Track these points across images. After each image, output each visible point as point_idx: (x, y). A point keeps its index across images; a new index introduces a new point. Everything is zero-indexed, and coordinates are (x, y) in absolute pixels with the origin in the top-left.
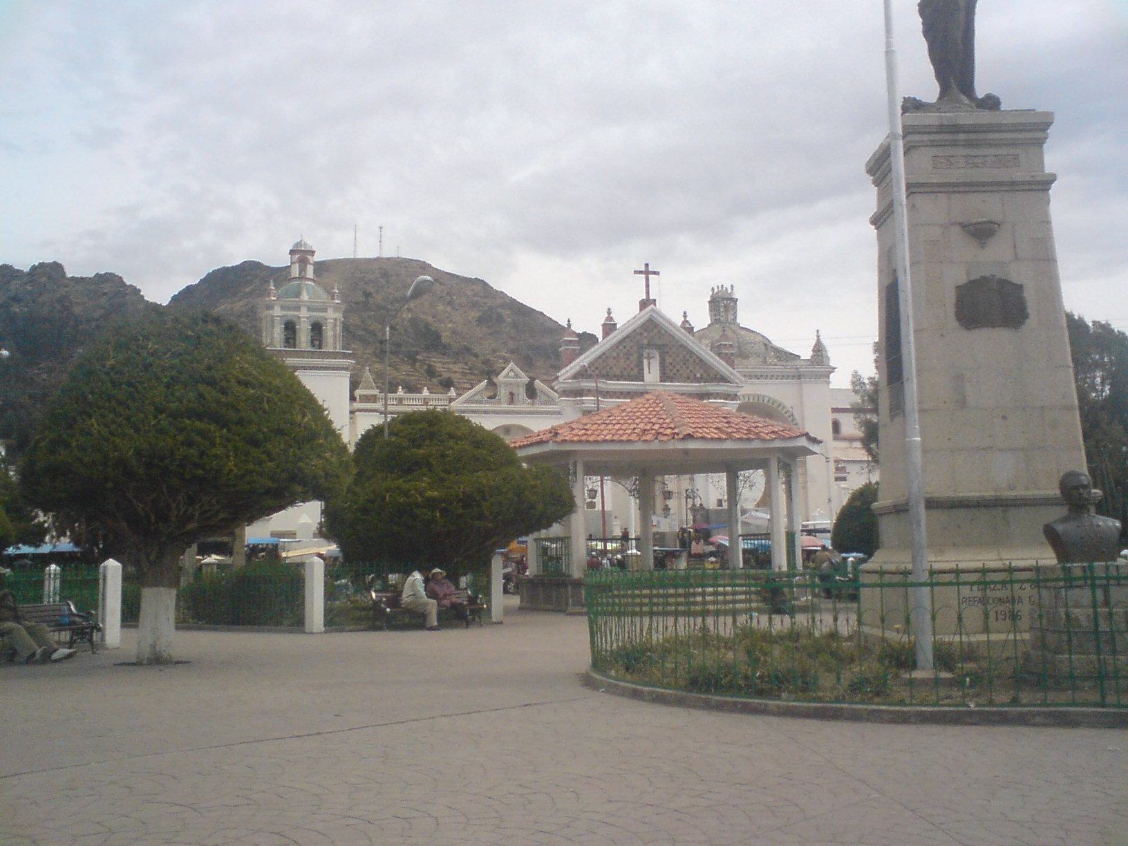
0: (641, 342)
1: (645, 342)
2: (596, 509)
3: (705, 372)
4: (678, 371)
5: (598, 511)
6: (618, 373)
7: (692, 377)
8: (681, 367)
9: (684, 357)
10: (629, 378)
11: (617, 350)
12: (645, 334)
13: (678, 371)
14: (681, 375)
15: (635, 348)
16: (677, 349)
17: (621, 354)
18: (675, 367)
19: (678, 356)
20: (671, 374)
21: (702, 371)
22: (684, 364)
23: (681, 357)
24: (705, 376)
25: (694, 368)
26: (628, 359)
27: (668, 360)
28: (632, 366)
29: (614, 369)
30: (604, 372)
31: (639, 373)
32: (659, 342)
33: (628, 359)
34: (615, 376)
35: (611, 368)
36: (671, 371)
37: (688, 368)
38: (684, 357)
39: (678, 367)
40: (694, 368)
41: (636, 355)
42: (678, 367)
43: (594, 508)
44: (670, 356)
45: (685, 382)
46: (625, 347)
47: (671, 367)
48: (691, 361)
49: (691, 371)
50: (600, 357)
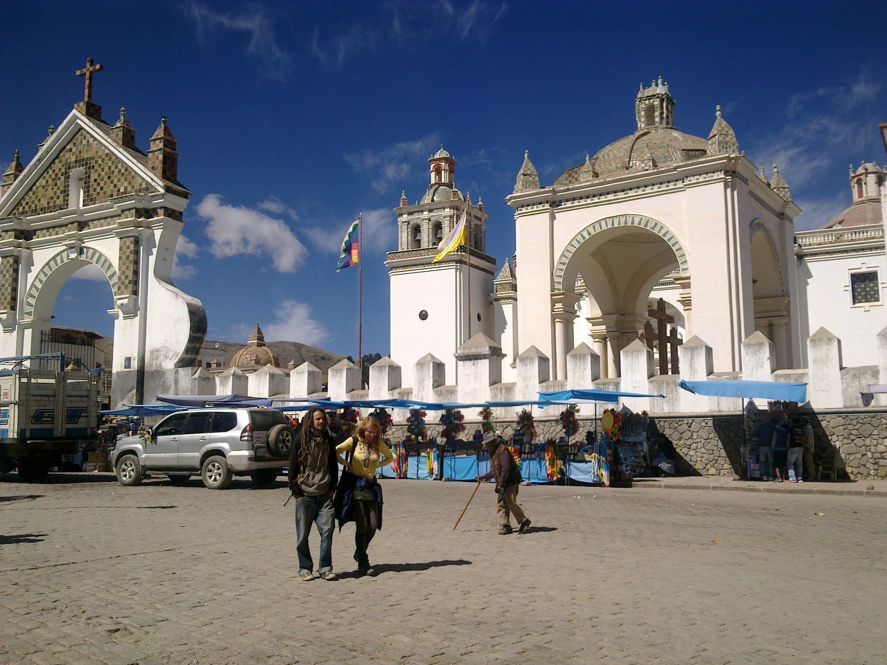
1: (73, 159)
9: (110, 168)
13: (102, 189)
14: (105, 193)
15: (63, 170)
17: (50, 182)
19: (103, 170)
22: (109, 178)
25: (119, 180)
27: (94, 176)
33: (56, 185)
35: (39, 200)
37: (112, 182)
38: (110, 168)
39: (102, 184)
40: (119, 180)
50: (31, 189)
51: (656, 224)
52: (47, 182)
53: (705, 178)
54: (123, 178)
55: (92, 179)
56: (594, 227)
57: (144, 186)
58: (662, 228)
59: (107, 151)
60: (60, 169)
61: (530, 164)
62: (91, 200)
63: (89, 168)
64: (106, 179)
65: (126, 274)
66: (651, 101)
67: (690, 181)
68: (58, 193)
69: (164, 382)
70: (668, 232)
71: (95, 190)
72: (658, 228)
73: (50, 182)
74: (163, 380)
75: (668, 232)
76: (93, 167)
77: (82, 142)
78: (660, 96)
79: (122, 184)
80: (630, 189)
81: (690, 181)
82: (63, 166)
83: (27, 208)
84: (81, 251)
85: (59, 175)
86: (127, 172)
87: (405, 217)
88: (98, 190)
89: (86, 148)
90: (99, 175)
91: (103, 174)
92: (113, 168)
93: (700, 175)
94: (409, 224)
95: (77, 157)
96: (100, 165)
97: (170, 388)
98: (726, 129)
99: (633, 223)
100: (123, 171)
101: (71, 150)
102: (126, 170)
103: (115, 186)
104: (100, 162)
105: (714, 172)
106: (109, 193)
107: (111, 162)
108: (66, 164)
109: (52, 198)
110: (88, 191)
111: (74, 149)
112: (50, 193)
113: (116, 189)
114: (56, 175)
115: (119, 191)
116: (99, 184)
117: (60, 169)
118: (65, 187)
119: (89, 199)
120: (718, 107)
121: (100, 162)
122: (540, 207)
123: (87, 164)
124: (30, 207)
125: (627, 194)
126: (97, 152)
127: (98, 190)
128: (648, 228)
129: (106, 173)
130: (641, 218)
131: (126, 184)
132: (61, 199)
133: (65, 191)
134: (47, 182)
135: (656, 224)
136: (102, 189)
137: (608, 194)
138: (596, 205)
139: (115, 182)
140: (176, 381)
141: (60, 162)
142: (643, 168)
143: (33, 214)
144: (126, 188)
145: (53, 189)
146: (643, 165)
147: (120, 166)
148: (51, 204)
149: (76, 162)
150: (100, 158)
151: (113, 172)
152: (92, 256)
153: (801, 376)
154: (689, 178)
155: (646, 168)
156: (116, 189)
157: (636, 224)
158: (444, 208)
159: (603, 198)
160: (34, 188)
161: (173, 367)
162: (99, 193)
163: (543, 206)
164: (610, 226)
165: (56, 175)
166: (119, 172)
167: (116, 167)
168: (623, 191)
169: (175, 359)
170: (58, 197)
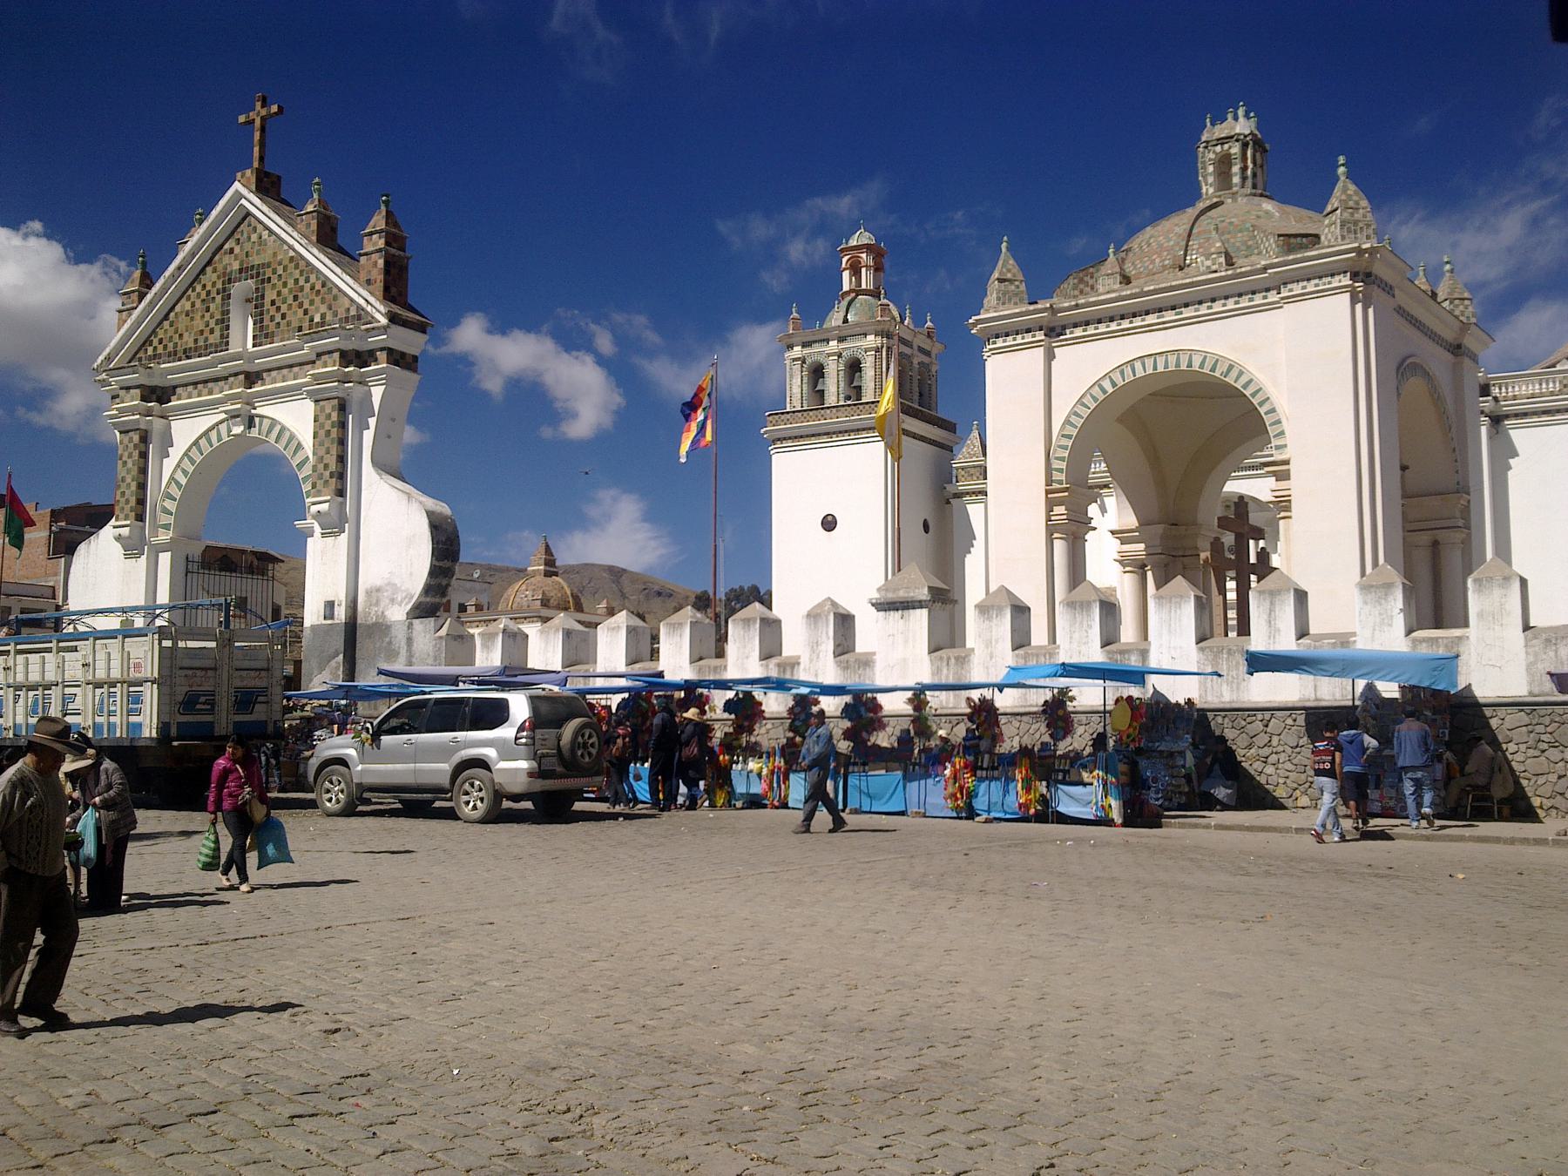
1: (236, 266)
9: (296, 281)
13: (283, 316)
14: (289, 324)
15: (220, 285)
17: (198, 304)
19: (285, 285)
22: (296, 298)
25: (312, 302)
27: (270, 295)
33: (208, 310)
35: (181, 336)
37: (301, 305)
38: (296, 281)
39: (284, 308)
40: (312, 302)
50: (166, 317)
51: (1231, 367)
52: (193, 305)
53: (1317, 285)
54: (317, 300)
55: (267, 301)
56: (1122, 373)
57: (353, 312)
58: (1241, 373)
59: (292, 253)
60: (214, 284)
61: (1011, 262)
62: (266, 336)
63: (263, 281)
65: (325, 462)
66: (1226, 146)
67: (1291, 290)
69: (390, 643)
70: (1251, 381)
72: (1234, 374)
73: (198, 304)
74: (387, 640)
75: (1251, 381)
77: (249, 238)
78: (1242, 137)
79: (317, 310)
80: (1186, 305)
81: (1291, 290)
82: (219, 278)
83: (160, 350)
84: (250, 423)
85: (213, 294)
86: (325, 289)
87: (797, 351)
88: (278, 319)
89: (256, 248)
90: (279, 294)
91: (285, 291)
92: (301, 282)
93: (1309, 280)
94: (804, 362)
95: (242, 263)
96: (280, 276)
97: (399, 653)
98: (1355, 198)
99: (1190, 365)
100: (318, 287)
101: (232, 251)
102: (324, 285)
103: (306, 312)
104: (280, 271)
105: (1332, 275)
106: (295, 324)
107: (298, 271)
108: (224, 274)
109: (202, 332)
110: (262, 321)
111: (237, 250)
112: (199, 324)
114: (208, 293)
115: (312, 320)
116: (278, 309)
117: (214, 284)
119: (262, 336)
120: (1342, 160)
121: (280, 271)
122: (1028, 338)
123: (258, 274)
124: (165, 347)
125: (1181, 313)
126: (275, 254)
127: (278, 319)
128: (1217, 374)
129: (291, 291)
130: (1205, 357)
131: (323, 309)
132: (217, 333)
133: (223, 321)
134: (193, 305)
135: (1231, 367)
136: (283, 316)
137: (1147, 313)
138: (1125, 333)
140: (410, 641)
141: (215, 271)
142: (1208, 267)
143: (171, 359)
144: (323, 316)
145: (203, 316)
146: (1208, 263)
147: (313, 278)
148: (201, 343)
149: (241, 271)
150: (280, 264)
151: (302, 288)
153: (1456, 640)
154: (1289, 286)
155: (1214, 268)
157: (1196, 367)
158: (865, 335)
159: (1138, 322)
160: (172, 314)
161: (405, 617)
162: (279, 323)
163: (1034, 336)
164: (1150, 371)
165: (208, 293)
166: (312, 288)
167: (307, 281)
168: (1173, 308)
169: (407, 604)
170: (212, 331)
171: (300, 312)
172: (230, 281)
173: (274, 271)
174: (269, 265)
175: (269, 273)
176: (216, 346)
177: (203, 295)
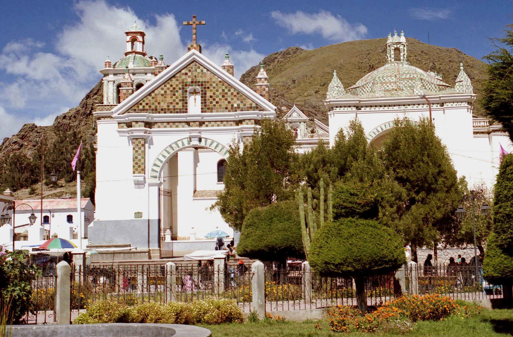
0: (185, 81)
1: (189, 80)
2: (142, 218)
3: (242, 102)
4: (217, 102)
5: (144, 220)
6: (165, 106)
7: (229, 107)
8: (220, 99)
9: (223, 90)
10: (175, 110)
11: (165, 88)
12: (189, 74)
13: (217, 102)
14: (220, 106)
15: (181, 86)
16: (217, 85)
17: (168, 92)
18: (214, 99)
19: (217, 91)
20: (211, 106)
21: (239, 102)
22: (223, 96)
23: (220, 91)
24: (241, 106)
25: (232, 99)
26: (174, 95)
27: (209, 94)
28: (177, 100)
29: (162, 104)
30: (153, 107)
31: (183, 106)
32: (201, 80)
33: (174, 95)
34: (162, 110)
35: (159, 103)
36: (211, 103)
37: (226, 99)
38: (223, 90)
39: (217, 99)
40: (232, 99)
41: (180, 91)
42: (217, 99)
43: (141, 217)
44: (211, 91)
45: (223, 112)
46: (171, 86)
47: (211, 100)
48: (229, 93)
49: (229, 102)
50: (150, 95)
52: (165, 92)
53: (456, 105)
54: (235, 99)
56: (385, 126)
57: (254, 105)
59: (220, 80)
63: (205, 88)
64: (221, 97)
67: (447, 105)
68: (177, 100)
71: (211, 103)
73: (168, 92)
76: (208, 88)
77: (196, 71)
79: (235, 102)
80: (409, 105)
81: (447, 105)
83: (147, 107)
84: (200, 140)
85: (177, 89)
87: (111, 77)
88: (214, 103)
90: (214, 94)
91: (217, 93)
92: (226, 91)
93: (454, 103)
94: (114, 82)
95: (192, 79)
100: (235, 93)
101: (186, 74)
102: (238, 94)
103: (229, 102)
104: (214, 85)
105: (462, 102)
106: (224, 106)
108: (183, 82)
110: (205, 103)
111: (189, 74)
113: (230, 105)
114: (174, 88)
115: (232, 106)
118: (183, 97)
119: (205, 107)
122: (349, 109)
123: (202, 85)
125: (407, 107)
131: (239, 102)
134: (165, 92)
137: (394, 106)
138: (386, 112)
139: (229, 99)
141: (177, 80)
143: (154, 112)
144: (238, 105)
147: (232, 90)
148: (171, 107)
149: (192, 82)
151: (227, 93)
152: (211, 144)
154: (447, 104)
156: (230, 105)
158: (146, 74)
159: (391, 108)
160: (153, 95)
163: (352, 109)
166: (232, 94)
168: (404, 105)
171: (226, 102)
172: (186, 85)
173: (211, 85)
174: (208, 82)
175: (208, 85)
176: (180, 109)
177: (171, 89)
